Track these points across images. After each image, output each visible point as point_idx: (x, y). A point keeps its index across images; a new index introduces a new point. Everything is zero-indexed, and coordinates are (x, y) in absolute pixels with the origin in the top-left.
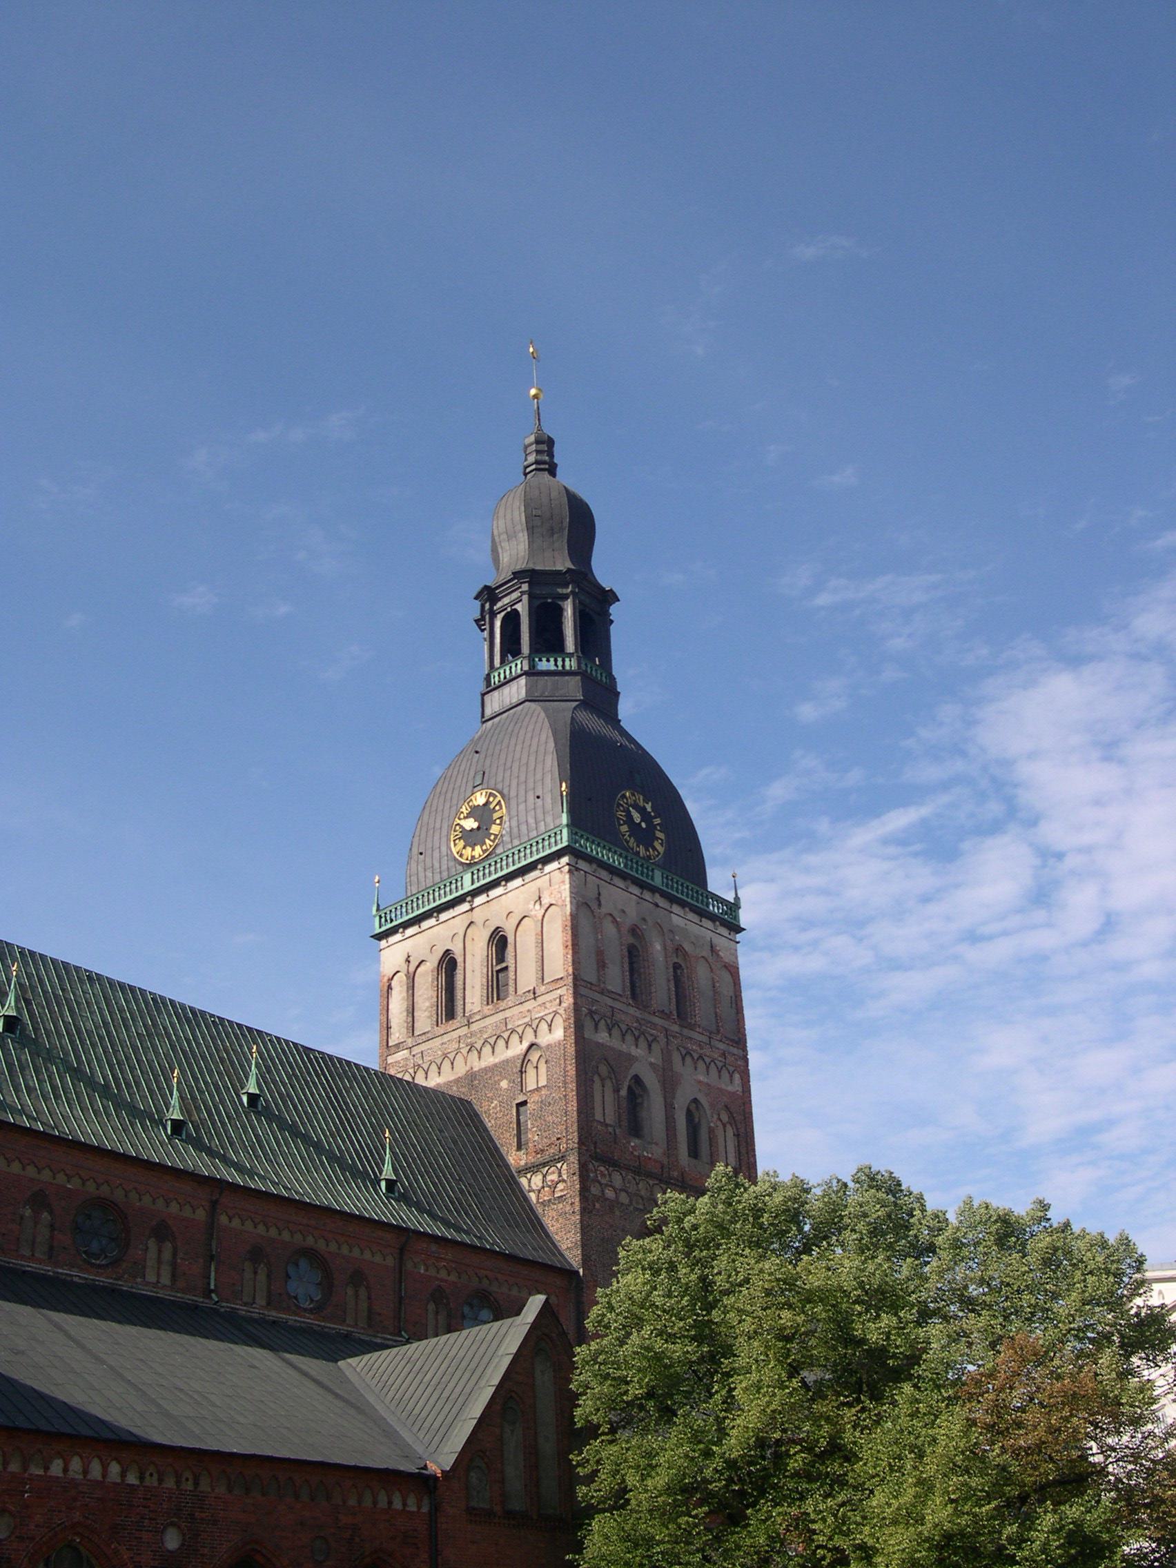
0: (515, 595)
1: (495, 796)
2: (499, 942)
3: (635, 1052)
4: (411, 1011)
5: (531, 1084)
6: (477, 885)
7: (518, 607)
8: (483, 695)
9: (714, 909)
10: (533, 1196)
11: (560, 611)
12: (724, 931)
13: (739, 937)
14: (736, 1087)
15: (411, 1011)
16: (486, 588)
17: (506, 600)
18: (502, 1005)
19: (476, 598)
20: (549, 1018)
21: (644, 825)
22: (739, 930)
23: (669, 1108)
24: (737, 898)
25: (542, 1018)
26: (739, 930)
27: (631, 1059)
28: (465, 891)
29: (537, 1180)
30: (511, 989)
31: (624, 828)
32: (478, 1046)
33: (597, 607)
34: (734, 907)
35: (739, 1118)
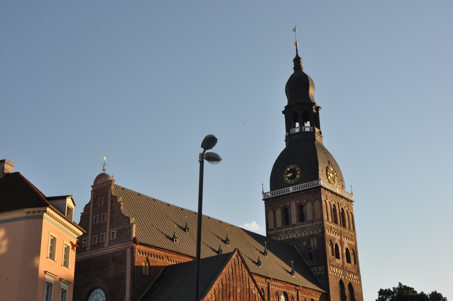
2: (301, 207)
3: (336, 237)
4: (275, 221)
5: (312, 245)
10: (314, 273)
13: (353, 203)
14: (354, 244)
15: (275, 221)
18: (303, 223)
20: (317, 229)
23: (342, 250)
25: (315, 228)
27: (335, 239)
29: (315, 269)
30: (305, 219)
32: (296, 233)
35: (355, 252)
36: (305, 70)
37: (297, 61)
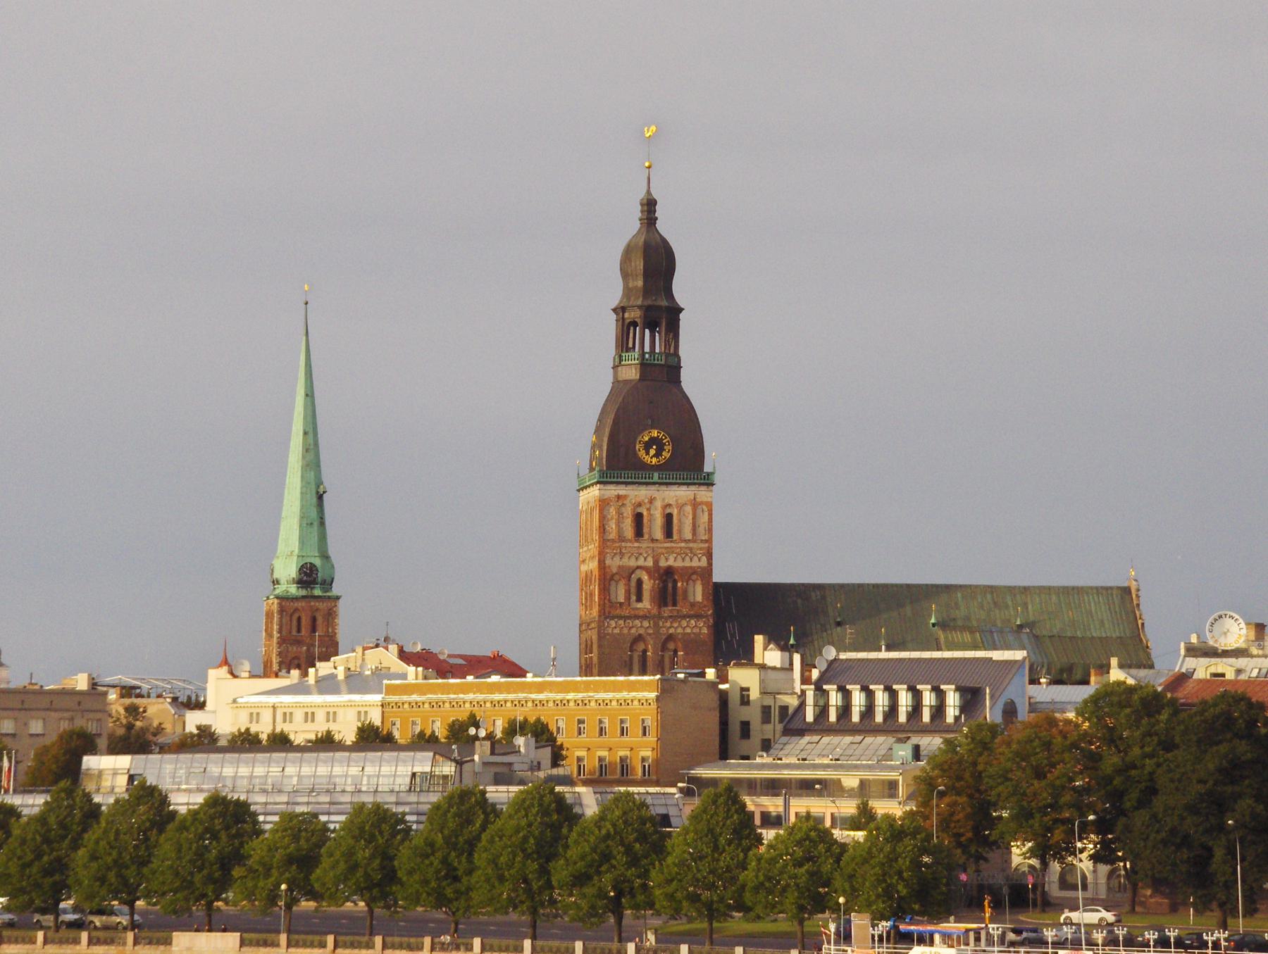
37: (650, 206)
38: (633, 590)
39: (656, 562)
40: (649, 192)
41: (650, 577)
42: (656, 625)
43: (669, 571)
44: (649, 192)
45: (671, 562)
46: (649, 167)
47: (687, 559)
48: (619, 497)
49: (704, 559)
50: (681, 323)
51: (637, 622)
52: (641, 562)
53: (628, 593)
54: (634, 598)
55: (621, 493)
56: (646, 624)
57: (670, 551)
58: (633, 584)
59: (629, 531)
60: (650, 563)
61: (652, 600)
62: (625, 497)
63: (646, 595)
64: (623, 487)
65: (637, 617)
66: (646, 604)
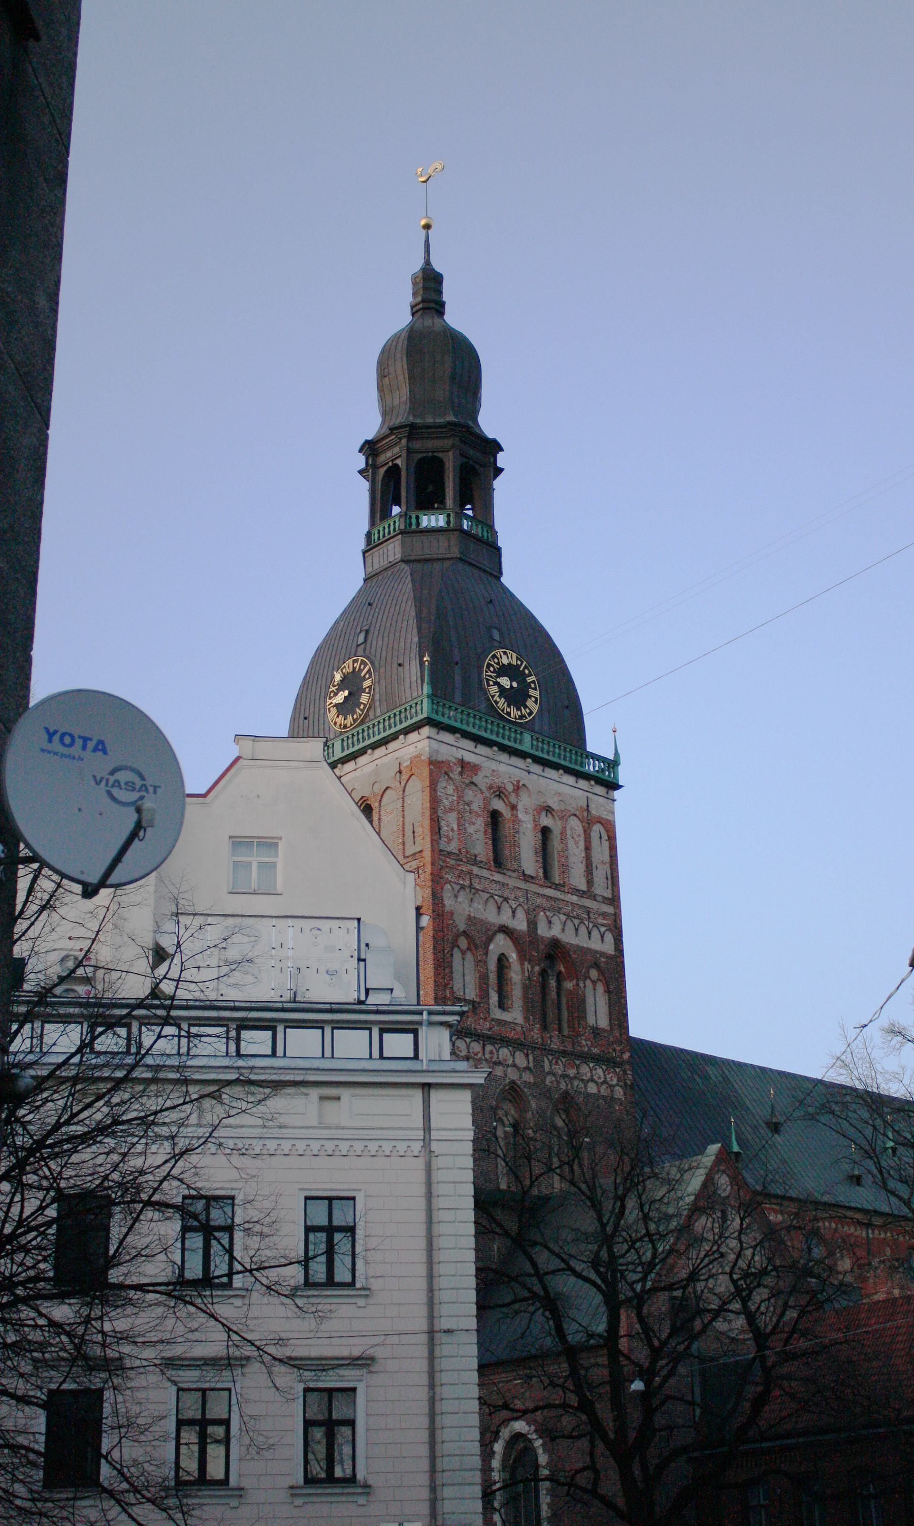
0: (396, 450)
1: (366, 664)
6: (346, 752)
7: (398, 462)
8: (364, 553)
9: (592, 767)
11: (441, 463)
12: (600, 790)
13: (617, 794)
16: (367, 442)
17: (389, 454)
19: (360, 451)
21: (515, 685)
22: (616, 786)
24: (616, 754)
26: (616, 786)
28: (336, 758)
31: (494, 689)
33: (479, 460)
34: (613, 764)
36: (456, 317)
38: (493, 978)
39: (532, 924)
40: (428, 262)
41: (522, 957)
42: (538, 1063)
43: (555, 952)
44: (428, 262)
45: (555, 932)
46: (427, 227)
47: (583, 930)
48: (463, 764)
49: (609, 937)
50: (496, 494)
51: (504, 1053)
52: (505, 918)
53: (483, 979)
54: (494, 997)
55: (469, 757)
56: (520, 1059)
57: (555, 907)
58: (492, 965)
59: (481, 847)
60: (520, 924)
61: (528, 1009)
62: (475, 768)
63: (516, 993)
64: (468, 744)
65: (504, 1041)
66: (515, 1015)
